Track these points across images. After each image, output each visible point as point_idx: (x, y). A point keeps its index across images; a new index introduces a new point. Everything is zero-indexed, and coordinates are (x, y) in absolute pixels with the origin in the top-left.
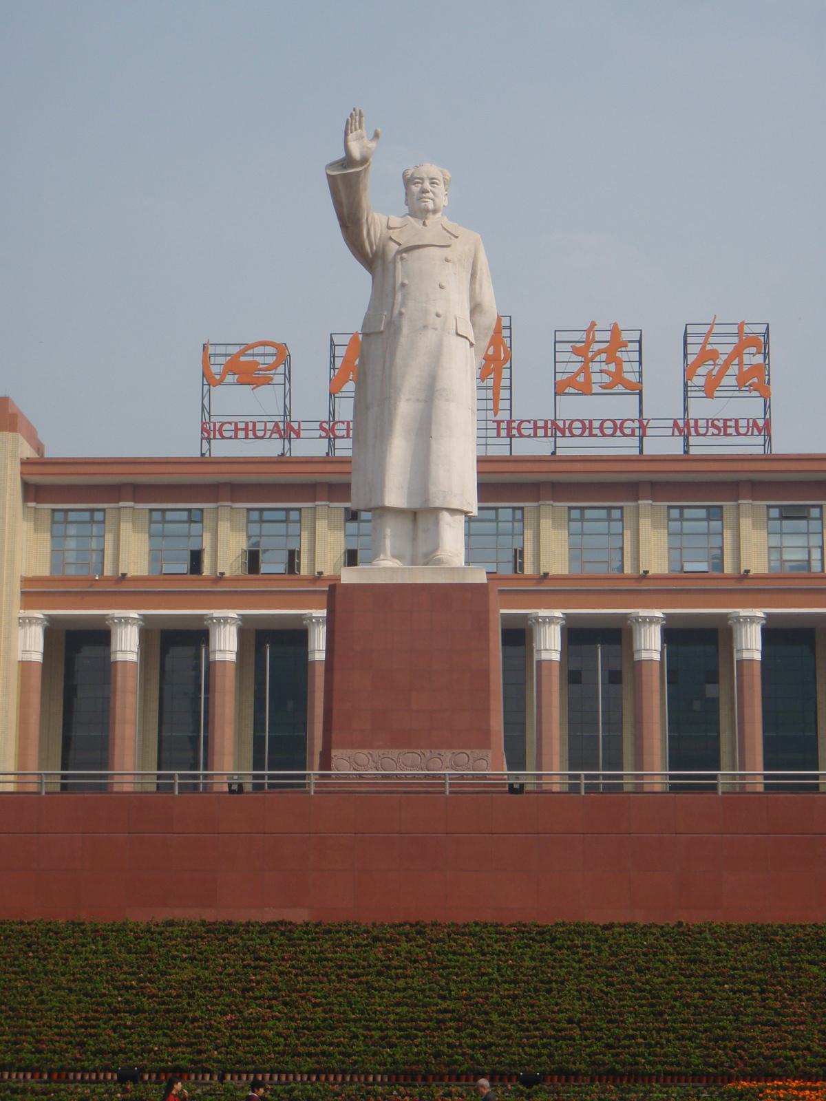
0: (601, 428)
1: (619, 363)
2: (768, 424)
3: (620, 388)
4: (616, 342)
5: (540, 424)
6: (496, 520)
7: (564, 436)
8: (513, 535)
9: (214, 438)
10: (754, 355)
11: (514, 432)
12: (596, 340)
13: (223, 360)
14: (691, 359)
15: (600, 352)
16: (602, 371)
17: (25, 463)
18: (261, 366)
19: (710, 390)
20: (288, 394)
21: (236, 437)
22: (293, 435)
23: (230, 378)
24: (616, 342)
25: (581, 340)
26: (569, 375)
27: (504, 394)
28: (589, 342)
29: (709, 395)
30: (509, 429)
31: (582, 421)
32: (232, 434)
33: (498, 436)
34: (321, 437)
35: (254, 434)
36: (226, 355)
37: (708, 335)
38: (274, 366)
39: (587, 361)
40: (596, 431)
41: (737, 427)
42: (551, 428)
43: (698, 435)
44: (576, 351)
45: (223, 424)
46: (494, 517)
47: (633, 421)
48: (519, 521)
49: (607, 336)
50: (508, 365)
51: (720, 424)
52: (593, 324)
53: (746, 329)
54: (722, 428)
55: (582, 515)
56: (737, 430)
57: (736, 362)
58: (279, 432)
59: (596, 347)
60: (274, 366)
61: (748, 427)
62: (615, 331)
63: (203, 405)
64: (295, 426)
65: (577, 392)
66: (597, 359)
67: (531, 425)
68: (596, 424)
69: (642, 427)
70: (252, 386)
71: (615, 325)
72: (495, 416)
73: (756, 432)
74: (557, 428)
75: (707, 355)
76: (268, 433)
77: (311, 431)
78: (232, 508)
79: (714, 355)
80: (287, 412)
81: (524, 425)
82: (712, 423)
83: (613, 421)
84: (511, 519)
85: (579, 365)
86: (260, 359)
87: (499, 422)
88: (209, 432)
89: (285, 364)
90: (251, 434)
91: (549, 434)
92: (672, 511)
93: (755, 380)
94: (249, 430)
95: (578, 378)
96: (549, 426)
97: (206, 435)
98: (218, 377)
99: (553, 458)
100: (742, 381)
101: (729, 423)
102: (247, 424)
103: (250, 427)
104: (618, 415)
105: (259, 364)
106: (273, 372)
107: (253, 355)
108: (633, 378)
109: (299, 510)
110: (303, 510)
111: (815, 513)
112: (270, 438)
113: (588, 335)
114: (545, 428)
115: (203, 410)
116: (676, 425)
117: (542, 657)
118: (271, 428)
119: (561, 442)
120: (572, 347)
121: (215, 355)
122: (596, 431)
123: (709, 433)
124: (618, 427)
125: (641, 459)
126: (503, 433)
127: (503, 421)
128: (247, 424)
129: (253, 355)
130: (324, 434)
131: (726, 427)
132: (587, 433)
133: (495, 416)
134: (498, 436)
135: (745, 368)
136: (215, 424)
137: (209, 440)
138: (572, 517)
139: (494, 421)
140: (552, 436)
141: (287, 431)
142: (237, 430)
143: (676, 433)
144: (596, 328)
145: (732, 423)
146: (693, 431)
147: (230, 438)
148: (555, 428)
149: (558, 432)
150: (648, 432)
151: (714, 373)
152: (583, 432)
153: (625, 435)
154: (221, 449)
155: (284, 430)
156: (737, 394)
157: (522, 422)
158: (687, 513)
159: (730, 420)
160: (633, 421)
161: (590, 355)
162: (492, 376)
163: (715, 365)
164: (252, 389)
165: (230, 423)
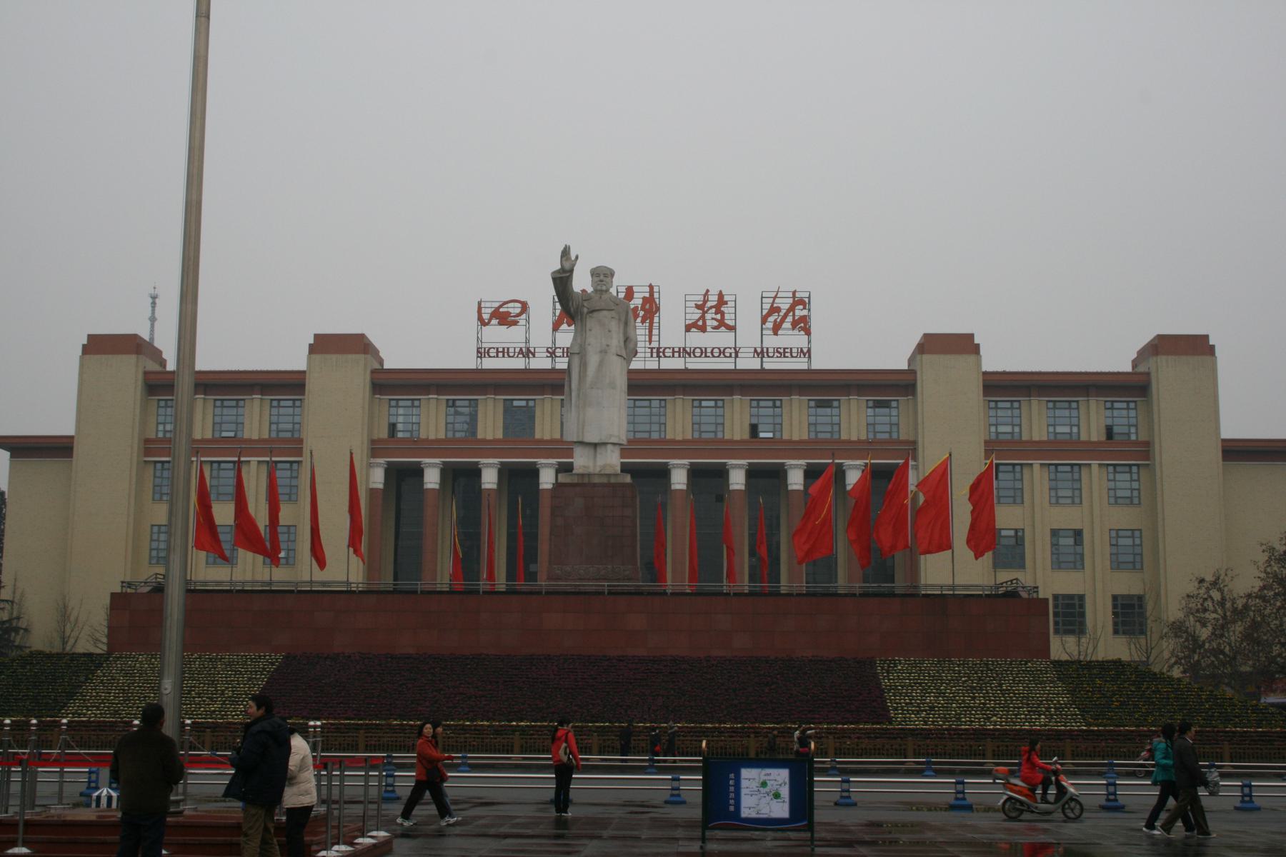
0: (712, 352)
1: (723, 314)
2: (809, 351)
3: (723, 329)
4: (721, 301)
5: (676, 350)
6: (650, 407)
7: (690, 357)
9: (485, 357)
10: (802, 310)
11: (661, 354)
13: (490, 311)
14: (765, 312)
15: (711, 307)
16: (713, 319)
17: (374, 372)
18: (512, 315)
19: (776, 329)
20: (528, 330)
21: (497, 356)
22: (531, 356)
23: (494, 321)
24: (721, 301)
26: (693, 321)
27: (655, 332)
28: (705, 301)
29: (776, 334)
30: (658, 352)
31: (700, 348)
33: (652, 356)
34: (547, 357)
35: (508, 354)
37: (775, 298)
38: (518, 315)
39: (704, 313)
40: (709, 354)
41: (791, 353)
43: (769, 357)
44: (698, 307)
47: (731, 348)
48: (662, 407)
49: (716, 298)
50: (657, 315)
51: (782, 351)
52: (708, 291)
53: (797, 295)
54: (783, 353)
56: (791, 355)
57: (791, 314)
58: (522, 353)
59: (709, 304)
60: (518, 315)
61: (798, 352)
62: (721, 295)
63: (478, 337)
64: (532, 350)
66: (710, 311)
68: (709, 350)
69: (737, 353)
71: (721, 291)
73: (802, 356)
74: (686, 352)
75: (774, 310)
76: (516, 354)
77: (541, 353)
78: (495, 399)
79: (778, 310)
80: (527, 341)
81: (667, 350)
82: (777, 350)
83: (719, 349)
86: (511, 310)
87: (652, 349)
88: (481, 353)
90: (506, 354)
92: (753, 402)
93: (802, 325)
94: (505, 352)
97: (480, 355)
98: (486, 321)
100: (795, 324)
101: (786, 350)
102: (504, 349)
103: (506, 351)
104: (722, 345)
108: (731, 323)
109: (534, 400)
110: (536, 401)
111: (835, 404)
112: (517, 357)
114: (679, 352)
116: (756, 351)
119: (688, 360)
120: (696, 304)
122: (709, 354)
123: (775, 356)
124: (722, 352)
125: (736, 371)
126: (655, 355)
128: (504, 349)
130: (549, 355)
131: (785, 352)
133: (650, 344)
135: (796, 318)
137: (481, 357)
138: (695, 405)
141: (528, 353)
142: (498, 352)
143: (756, 356)
144: (709, 293)
145: (789, 350)
146: (765, 354)
147: (494, 357)
148: (684, 352)
150: (740, 355)
151: (778, 320)
153: (726, 357)
154: (489, 364)
156: (791, 332)
157: (666, 348)
158: (762, 403)
159: (787, 348)
160: (731, 348)
161: (706, 309)
163: (779, 316)
165: (494, 348)
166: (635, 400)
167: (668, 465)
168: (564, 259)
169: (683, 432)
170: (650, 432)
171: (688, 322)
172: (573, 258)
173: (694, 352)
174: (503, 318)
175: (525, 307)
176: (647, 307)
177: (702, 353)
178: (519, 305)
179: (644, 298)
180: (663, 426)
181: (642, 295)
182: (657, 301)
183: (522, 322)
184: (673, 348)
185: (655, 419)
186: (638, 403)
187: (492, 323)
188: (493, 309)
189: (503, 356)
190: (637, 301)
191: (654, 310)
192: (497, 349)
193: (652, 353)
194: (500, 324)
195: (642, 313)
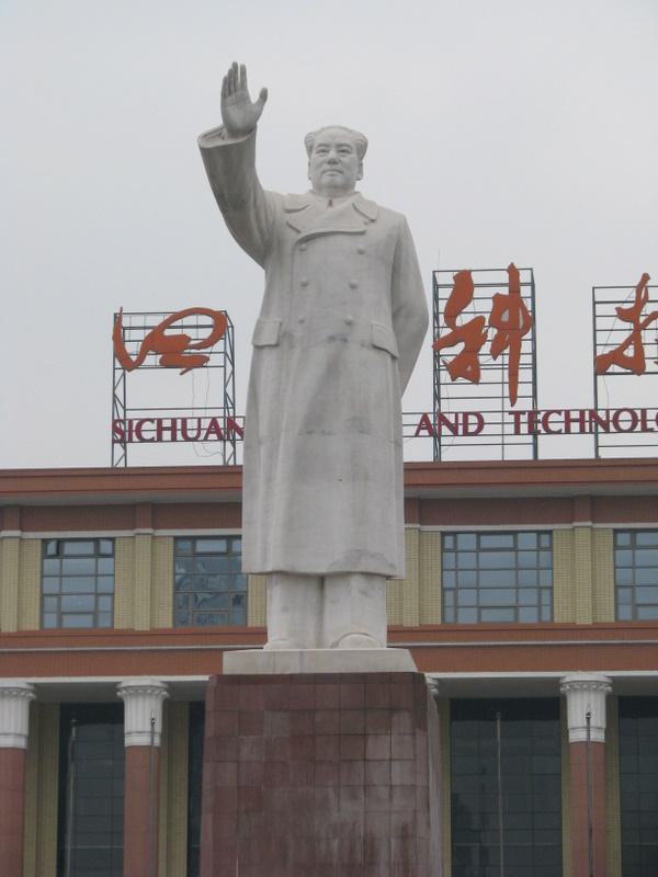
6: (515, 549)
7: (607, 431)
8: (538, 569)
9: (131, 441)
12: (650, 299)
13: (141, 335)
18: (192, 343)
21: (160, 439)
23: (152, 359)
25: (629, 299)
27: (525, 375)
28: (641, 302)
30: (532, 421)
31: (632, 411)
32: (154, 434)
33: (517, 432)
36: (145, 328)
39: (639, 328)
42: (591, 422)
44: (623, 315)
45: (142, 421)
46: (511, 545)
48: (545, 549)
50: (529, 335)
52: (646, 277)
55: (633, 540)
58: (217, 431)
63: (114, 396)
65: (623, 370)
67: (562, 418)
70: (180, 370)
72: (512, 406)
74: (599, 421)
76: (203, 433)
78: (154, 537)
81: (553, 417)
84: (535, 547)
85: (627, 334)
86: (190, 333)
87: (517, 414)
88: (124, 432)
89: (225, 339)
90: (179, 436)
91: (587, 430)
94: (176, 430)
95: (625, 353)
96: (587, 418)
97: (119, 437)
98: (134, 358)
99: (597, 464)
102: (174, 421)
103: (179, 426)
105: (190, 339)
106: (209, 350)
107: (182, 327)
112: (206, 439)
113: (638, 293)
114: (581, 421)
115: (114, 402)
117: (144, 740)
118: (207, 426)
119: (604, 439)
120: (617, 309)
121: (131, 328)
126: (524, 428)
127: (523, 413)
128: (174, 421)
129: (182, 327)
132: (639, 427)
133: (512, 406)
134: (517, 432)
136: (131, 422)
137: (123, 442)
138: (619, 543)
139: (511, 413)
140: (591, 432)
142: (160, 429)
144: (649, 283)
147: (152, 440)
148: (595, 421)
149: (599, 427)
152: (634, 426)
154: (142, 456)
155: (224, 429)
157: (549, 413)
161: (642, 319)
162: (507, 351)
164: (182, 374)
166: (479, 534)
167: (561, 685)
168: (229, 99)
169: (594, 609)
170: (516, 608)
171: (601, 351)
172: (254, 97)
173: (616, 421)
174: (172, 350)
175: (221, 324)
176: (505, 317)
177: (635, 421)
178: (208, 320)
179: (497, 299)
180: (546, 594)
181: (492, 292)
182: (528, 304)
183: (215, 360)
184: (567, 413)
185: (528, 577)
186: (486, 541)
187: (145, 363)
188: (149, 331)
189: (174, 439)
190: (481, 305)
191: (521, 322)
192: (160, 421)
193: (517, 424)
194: (165, 364)
195: (492, 333)
